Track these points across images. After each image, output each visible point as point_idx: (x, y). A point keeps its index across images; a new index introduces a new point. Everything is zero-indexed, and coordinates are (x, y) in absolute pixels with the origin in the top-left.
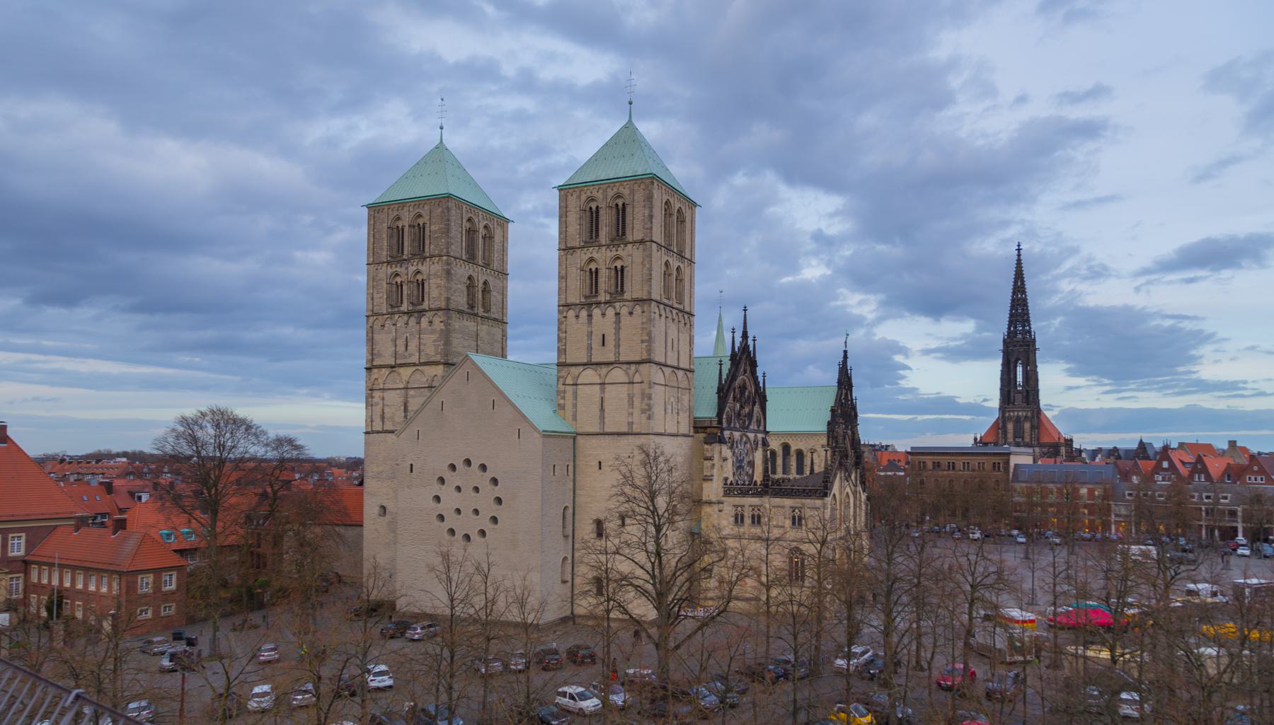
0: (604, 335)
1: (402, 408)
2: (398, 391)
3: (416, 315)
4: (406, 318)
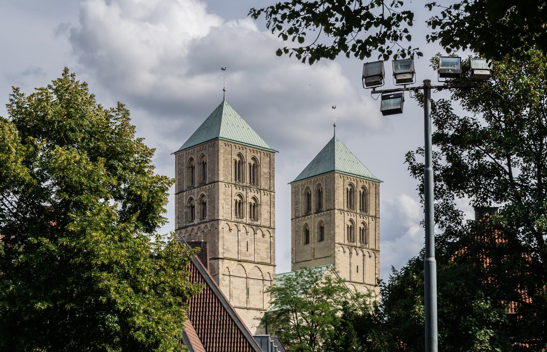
1: (246, 291)
2: (242, 279)
3: (254, 227)
4: (247, 227)
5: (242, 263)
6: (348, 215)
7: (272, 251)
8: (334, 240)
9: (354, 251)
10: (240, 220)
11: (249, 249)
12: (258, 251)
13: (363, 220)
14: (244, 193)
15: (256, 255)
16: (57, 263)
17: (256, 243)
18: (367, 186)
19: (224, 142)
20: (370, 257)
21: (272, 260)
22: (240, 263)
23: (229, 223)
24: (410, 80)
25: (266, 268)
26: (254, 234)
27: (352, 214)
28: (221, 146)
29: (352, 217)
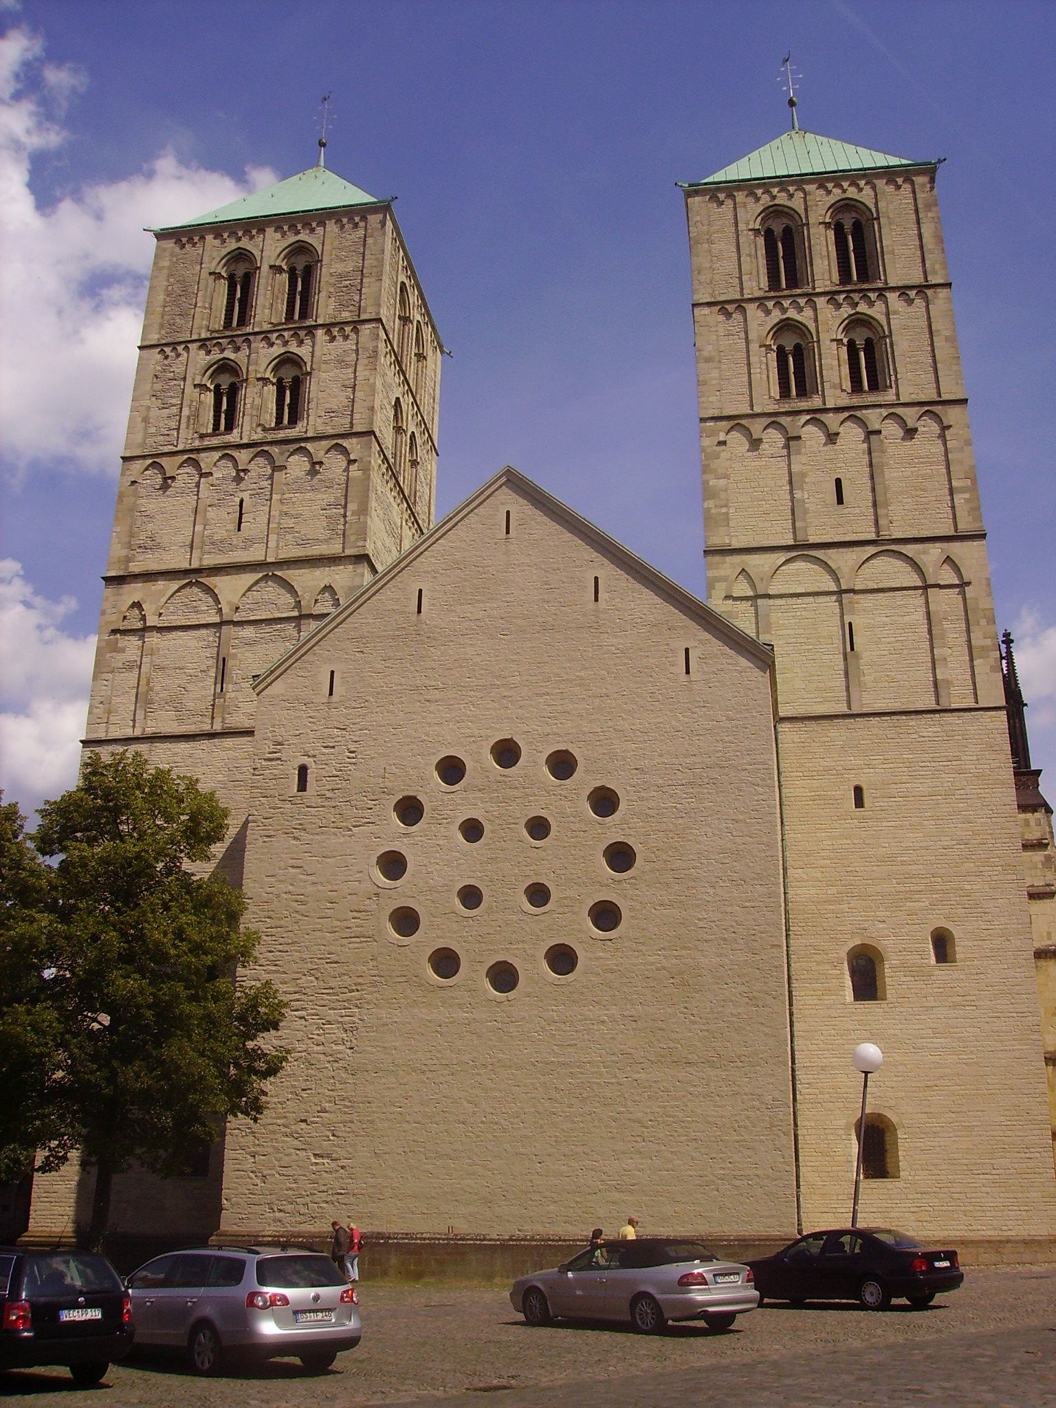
0: (838, 482)
14: (240, 357)
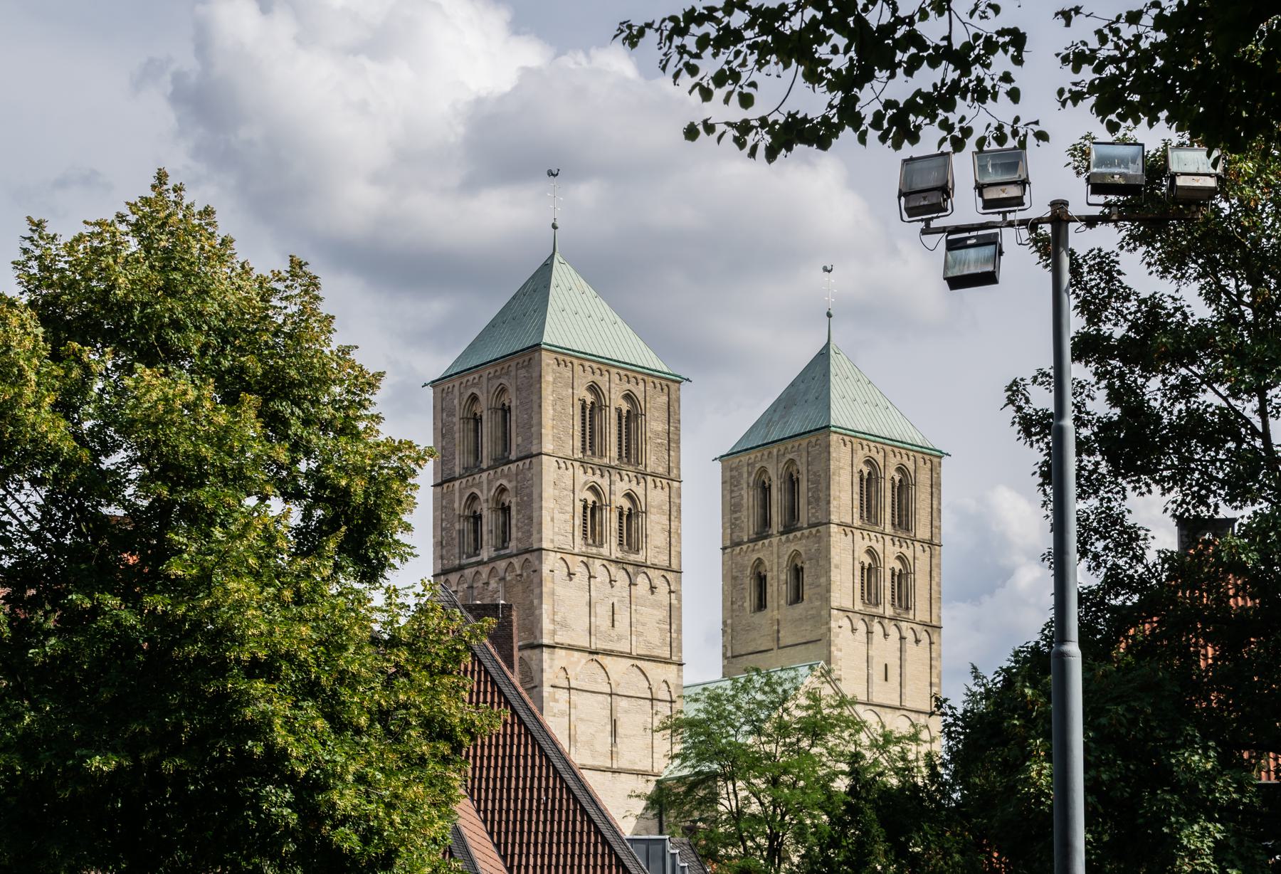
2: (600, 697)
3: (630, 569)
4: (613, 568)
5: (599, 657)
6: (863, 538)
7: (674, 627)
8: (828, 600)
9: (877, 628)
10: (594, 550)
11: (616, 623)
12: (640, 628)
13: (899, 550)
14: (604, 483)
15: (634, 637)
16: (141, 658)
17: (633, 607)
18: (910, 465)
19: (554, 355)
20: (917, 641)
21: (674, 650)
22: (595, 657)
23: (568, 557)
24: (1018, 201)
25: (659, 670)
26: (630, 585)
27: (872, 534)
28: (548, 365)
29: (873, 544)
